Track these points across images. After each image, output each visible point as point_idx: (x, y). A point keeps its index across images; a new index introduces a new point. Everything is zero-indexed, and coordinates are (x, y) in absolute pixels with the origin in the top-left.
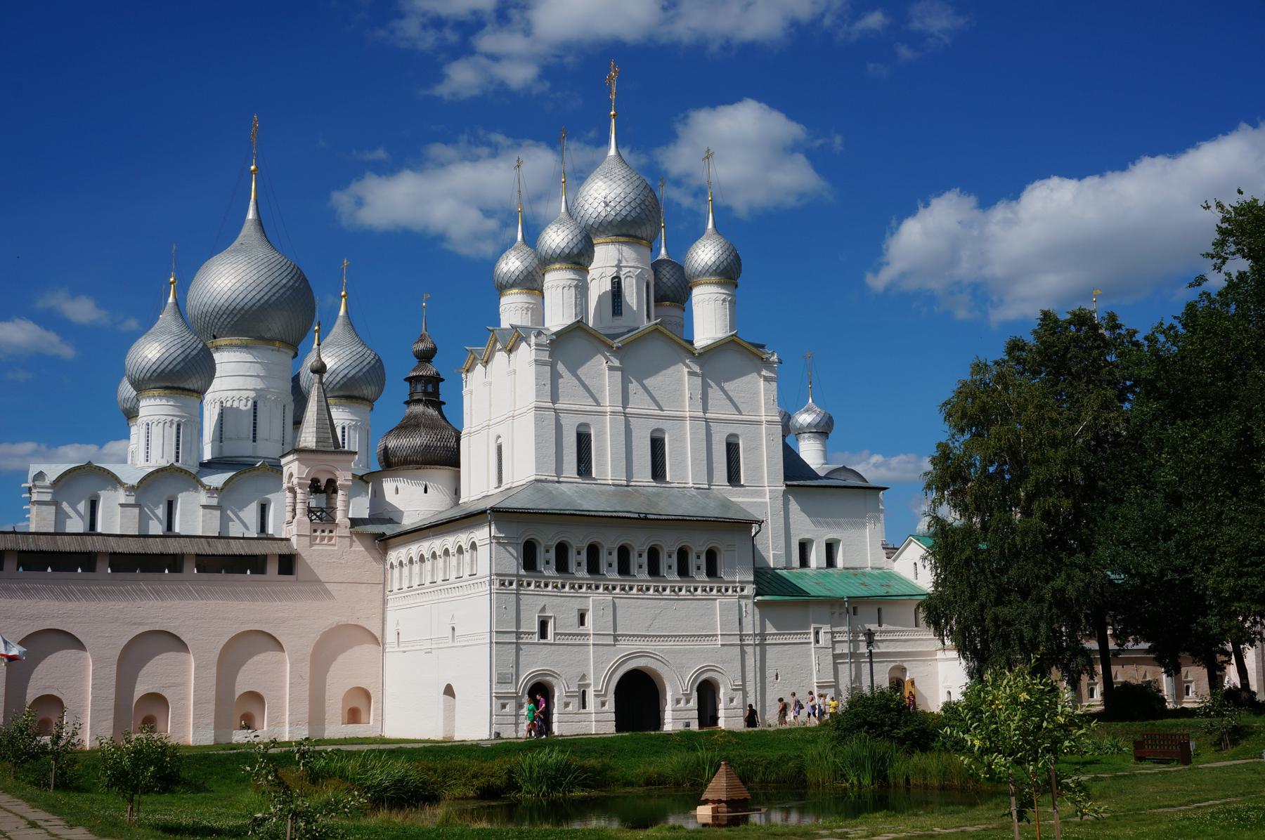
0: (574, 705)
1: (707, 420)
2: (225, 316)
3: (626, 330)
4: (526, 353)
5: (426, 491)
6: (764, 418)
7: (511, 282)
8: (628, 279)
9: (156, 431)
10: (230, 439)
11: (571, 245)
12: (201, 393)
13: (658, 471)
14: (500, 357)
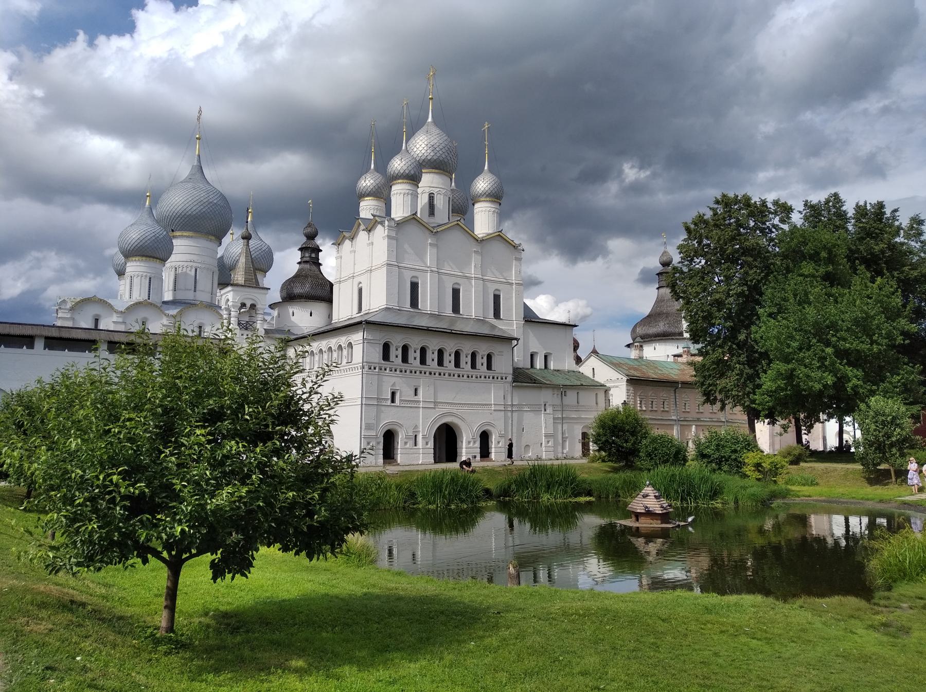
0: (410, 443)
1: (483, 280)
2: (179, 219)
3: (436, 225)
4: (380, 232)
5: (311, 315)
6: (514, 282)
7: (367, 192)
8: (439, 195)
9: (136, 281)
10: (180, 290)
11: (410, 168)
12: (164, 260)
13: (456, 308)
14: (362, 235)
